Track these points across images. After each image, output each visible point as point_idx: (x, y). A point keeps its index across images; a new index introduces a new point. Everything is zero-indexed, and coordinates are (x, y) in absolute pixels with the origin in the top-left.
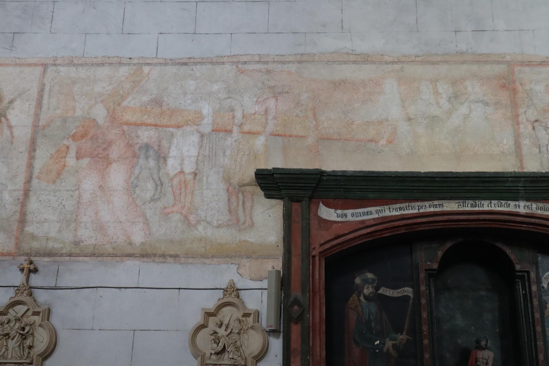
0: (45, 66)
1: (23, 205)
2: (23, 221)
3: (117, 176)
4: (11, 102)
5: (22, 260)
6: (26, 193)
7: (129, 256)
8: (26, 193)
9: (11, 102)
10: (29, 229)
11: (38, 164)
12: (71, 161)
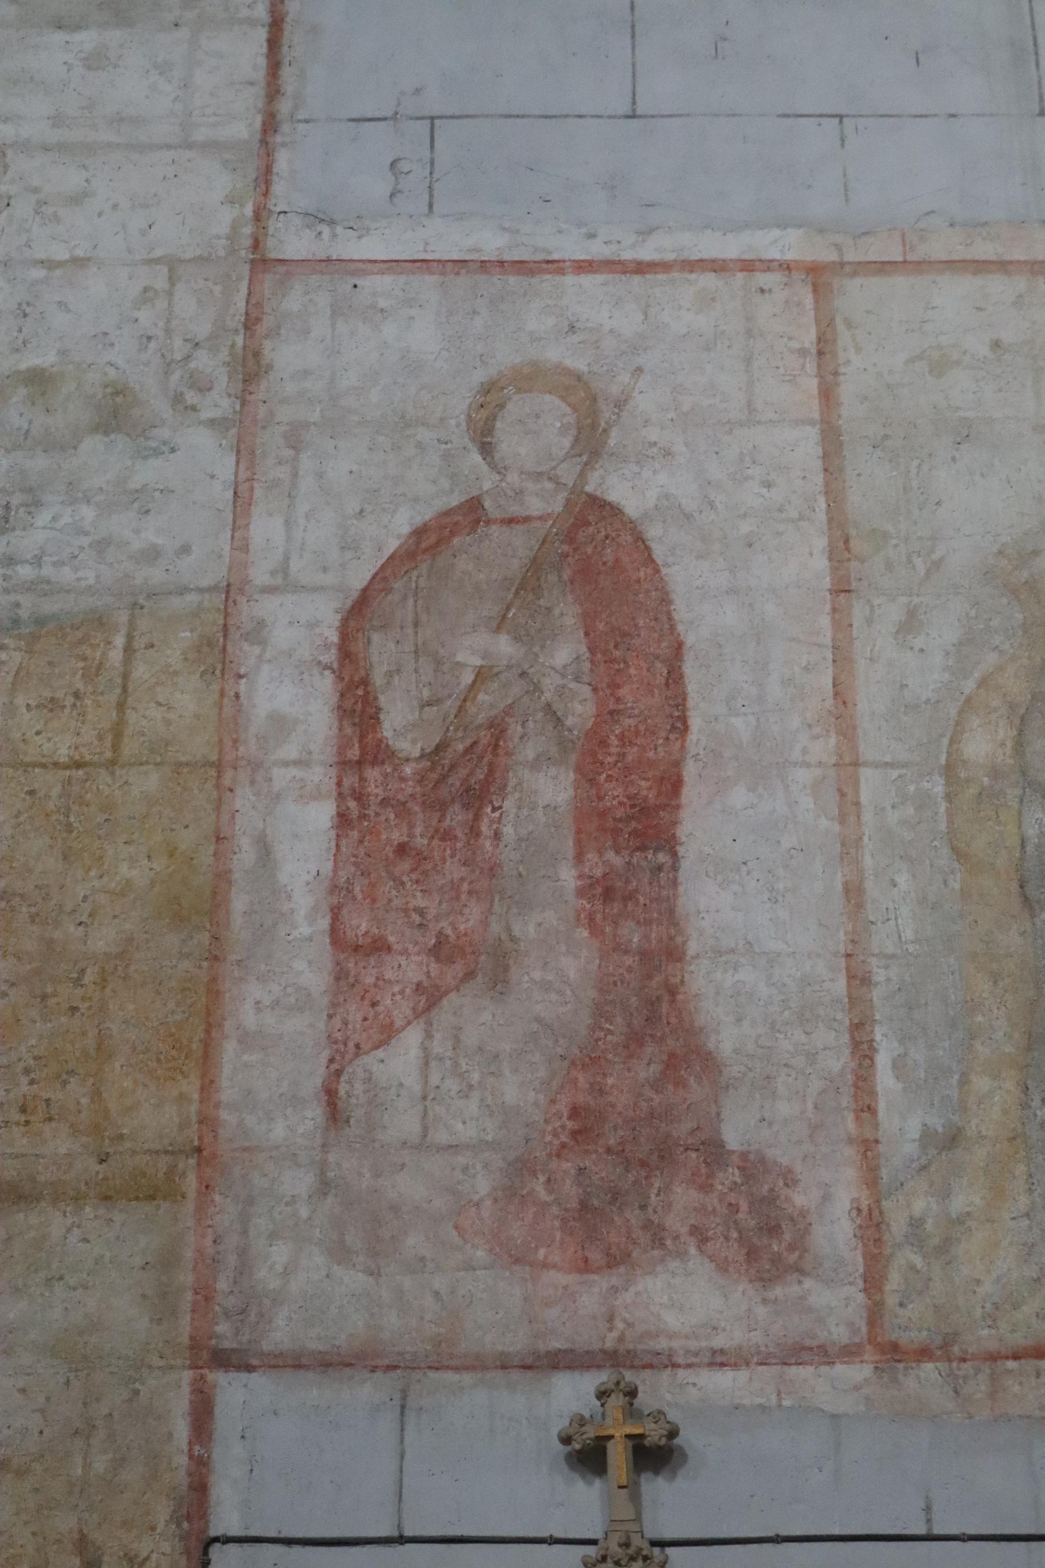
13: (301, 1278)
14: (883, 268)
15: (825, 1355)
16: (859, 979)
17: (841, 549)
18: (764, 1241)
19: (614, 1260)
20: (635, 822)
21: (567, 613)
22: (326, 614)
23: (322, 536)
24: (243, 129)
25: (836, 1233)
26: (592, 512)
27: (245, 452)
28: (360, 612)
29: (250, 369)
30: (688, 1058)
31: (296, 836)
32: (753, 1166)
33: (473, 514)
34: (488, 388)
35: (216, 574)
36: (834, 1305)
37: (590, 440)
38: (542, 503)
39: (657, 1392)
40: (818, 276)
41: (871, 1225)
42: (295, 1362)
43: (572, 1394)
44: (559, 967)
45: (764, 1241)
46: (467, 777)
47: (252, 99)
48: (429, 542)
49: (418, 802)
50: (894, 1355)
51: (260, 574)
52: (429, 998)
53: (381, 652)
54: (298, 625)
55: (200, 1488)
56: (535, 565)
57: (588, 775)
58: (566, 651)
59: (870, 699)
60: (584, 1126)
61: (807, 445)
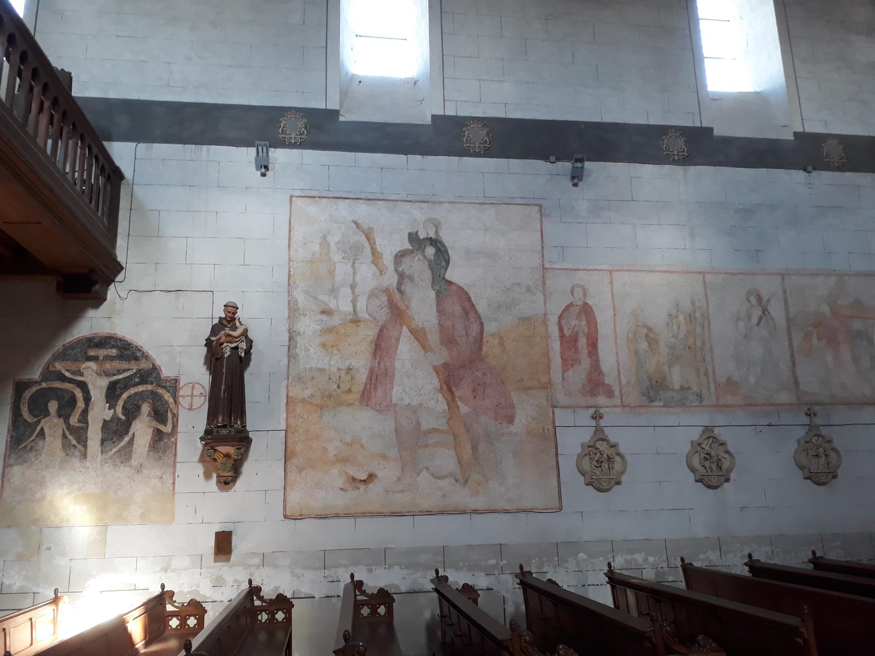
0: (783, 276)
1: (794, 372)
2: (796, 383)
3: (846, 354)
4: (768, 301)
5: (805, 408)
6: (794, 364)
7: (867, 404)
8: (794, 364)
9: (768, 301)
10: (801, 387)
11: (795, 344)
12: (815, 340)
13: (561, 397)
14: (618, 270)
15: (617, 406)
16: (618, 364)
17: (614, 310)
18: (610, 394)
19: (595, 395)
20: (593, 345)
21: (584, 318)
22: (556, 318)
23: (555, 308)
24: (540, 248)
25: (617, 393)
26: (586, 304)
27: (544, 294)
28: (560, 317)
29: (544, 283)
30: (601, 373)
31: (556, 345)
32: (608, 385)
33: (571, 304)
34: (572, 287)
35: (543, 312)
36: (617, 401)
37: (585, 295)
38: (580, 303)
39: (602, 411)
40: (610, 271)
41: (621, 392)
42: (562, 407)
43: (592, 411)
44: (586, 362)
45: (610, 394)
46: (575, 339)
47: (540, 242)
48: (567, 308)
49: (569, 342)
50: (624, 406)
51: (548, 312)
52: (572, 365)
53: (563, 322)
54: (553, 319)
55: (554, 421)
56: (580, 312)
57: (587, 338)
58: (584, 323)
59: (618, 330)
60: (590, 381)
61: (610, 295)
